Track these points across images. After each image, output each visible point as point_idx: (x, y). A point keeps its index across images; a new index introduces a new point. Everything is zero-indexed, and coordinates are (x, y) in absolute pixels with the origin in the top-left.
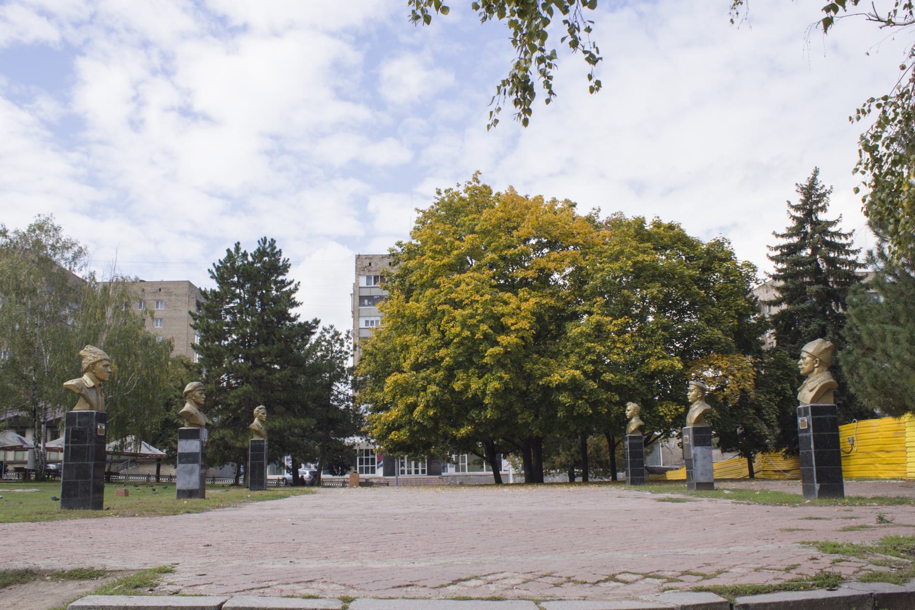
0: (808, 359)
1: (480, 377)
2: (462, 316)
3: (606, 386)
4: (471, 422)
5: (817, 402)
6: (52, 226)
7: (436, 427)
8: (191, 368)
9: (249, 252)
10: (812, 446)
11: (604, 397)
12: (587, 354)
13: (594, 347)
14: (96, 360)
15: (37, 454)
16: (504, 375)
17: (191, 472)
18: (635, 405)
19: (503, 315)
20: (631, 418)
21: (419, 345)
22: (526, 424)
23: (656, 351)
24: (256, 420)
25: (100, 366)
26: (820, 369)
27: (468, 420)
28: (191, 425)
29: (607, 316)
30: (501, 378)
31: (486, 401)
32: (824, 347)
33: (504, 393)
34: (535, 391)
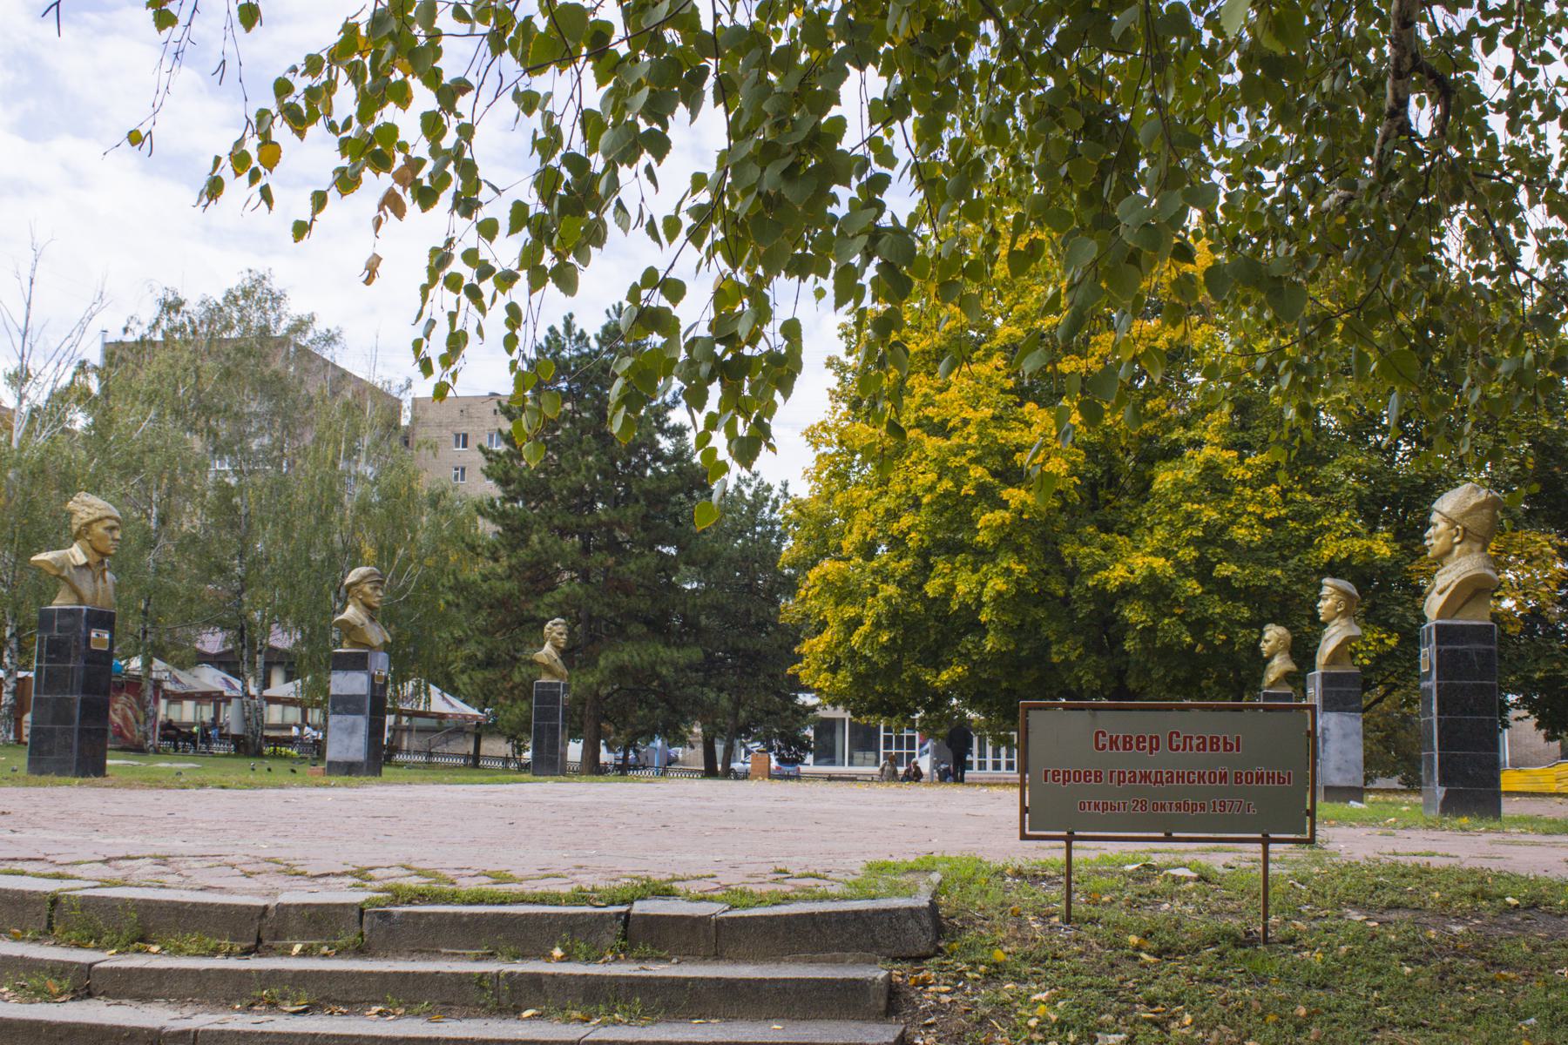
0: (1442, 526)
1: (975, 570)
2: (939, 449)
3: (1225, 588)
4: (965, 657)
5: (1452, 617)
6: (270, 291)
7: (894, 670)
8: (479, 550)
9: (590, 333)
10: (1435, 708)
11: (1218, 610)
12: (1185, 527)
13: (1200, 512)
14: (91, 518)
15: (247, 708)
16: (1013, 566)
17: (351, 731)
18: (1281, 630)
19: (1020, 448)
20: (1271, 657)
21: (871, 509)
22: (1068, 665)
23: (1337, 520)
24: (548, 647)
25: (99, 529)
26: (1465, 546)
27: (961, 655)
28: (354, 644)
29: (1227, 448)
30: (1008, 572)
31: (983, 618)
32: (1473, 501)
33: (1018, 600)
34: (1082, 597)
